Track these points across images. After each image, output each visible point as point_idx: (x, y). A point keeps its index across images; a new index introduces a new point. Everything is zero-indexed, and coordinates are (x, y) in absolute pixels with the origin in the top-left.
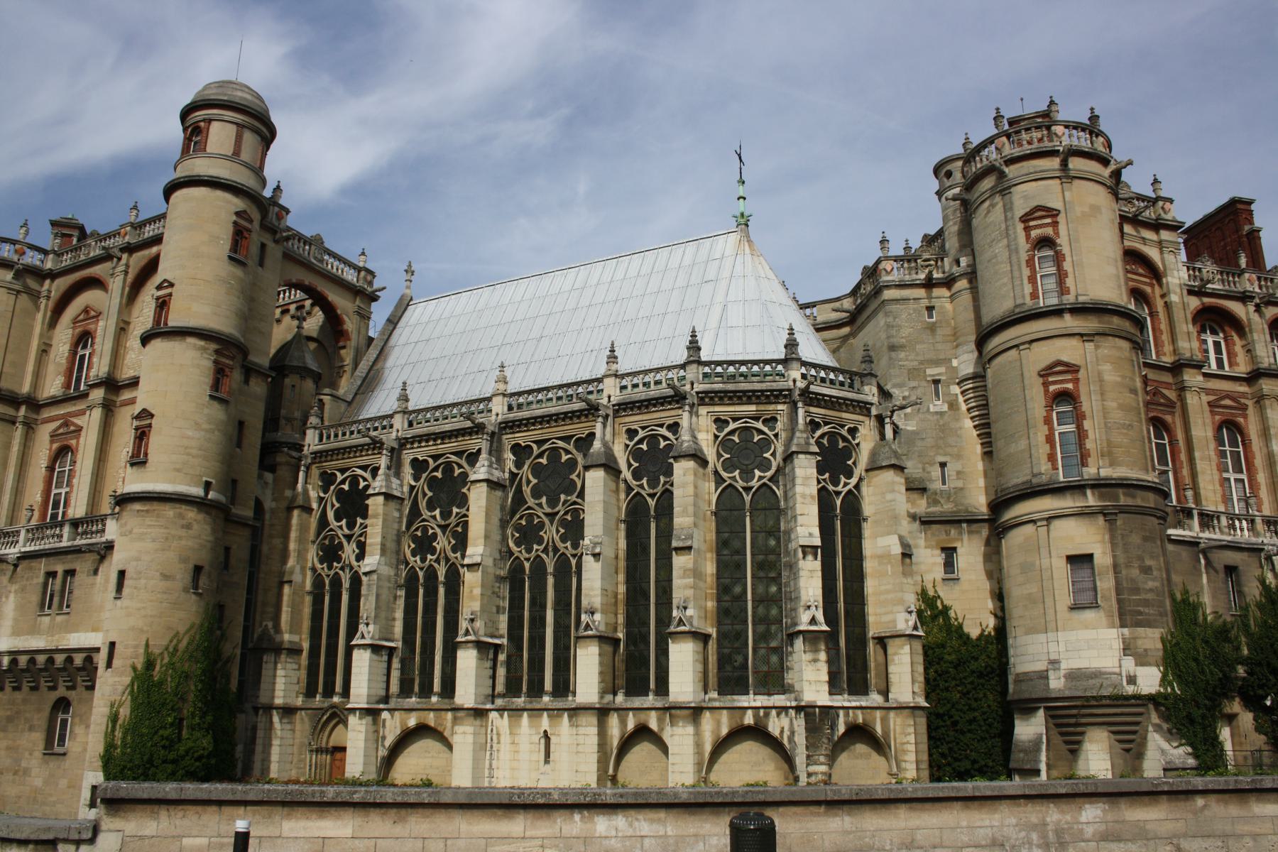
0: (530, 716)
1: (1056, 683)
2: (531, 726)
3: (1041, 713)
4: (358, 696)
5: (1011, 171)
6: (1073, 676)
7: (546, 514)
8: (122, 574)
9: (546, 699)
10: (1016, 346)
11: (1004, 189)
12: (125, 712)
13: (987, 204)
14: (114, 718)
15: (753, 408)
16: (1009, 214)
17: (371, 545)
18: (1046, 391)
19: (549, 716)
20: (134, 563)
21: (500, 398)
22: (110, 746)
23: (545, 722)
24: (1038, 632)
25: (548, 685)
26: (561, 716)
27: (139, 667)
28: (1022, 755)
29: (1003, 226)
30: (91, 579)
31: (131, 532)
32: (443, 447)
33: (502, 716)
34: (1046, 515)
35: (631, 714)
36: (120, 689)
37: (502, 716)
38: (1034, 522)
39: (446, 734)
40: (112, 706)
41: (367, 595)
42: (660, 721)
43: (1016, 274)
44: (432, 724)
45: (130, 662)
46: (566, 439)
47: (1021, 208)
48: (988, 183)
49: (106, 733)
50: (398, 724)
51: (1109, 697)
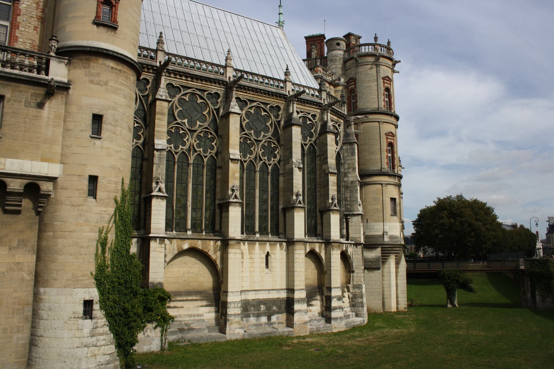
0: (260, 244)
1: (386, 239)
2: (260, 250)
3: (379, 249)
4: (158, 229)
5: (381, 59)
6: (391, 237)
7: (255, 140)
8: (97, 119)
9: (258, 235)
10: (379, 122)
11: (377, 64)
12: (111, 237)
13: (370, 66)
14: (103, 243)
15: (336, 118)
16: (379, 74)
17: (158, 132)
18: (387, 141)
19: (270, 245)
20: (112, 112)
21: (232, 69)
22: (101, 268)
23: (268, 247)
24: (379, 221)
25: (257, 229)
26: (276, 245)
27: (119, 199)
28: (370, 263)
29: (376, 77)
30: (33, 111)
31: (106, 84)
32: (190, 83)
33: (244, 244)
34: (386, 183)
35: (308, 244)
36: (107, 218)
37: (244, 244)
38: (382, 184)
39: (209, 253)
40: (100, 232)
41: (159, 165)
42: (320, 248)
43: (379, 96)
44: (200, 247)
45: (112, 195)
46: (267, 104)
47: (382, 75)
48: (371, 59)
49: (96, 255)
50: (175, 247)
51: (399, 245)
